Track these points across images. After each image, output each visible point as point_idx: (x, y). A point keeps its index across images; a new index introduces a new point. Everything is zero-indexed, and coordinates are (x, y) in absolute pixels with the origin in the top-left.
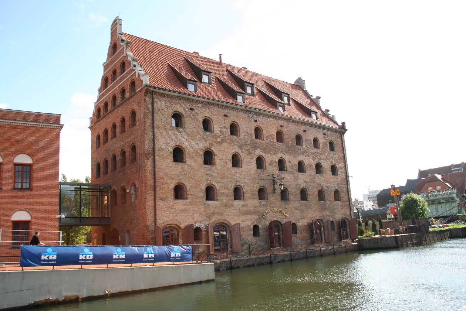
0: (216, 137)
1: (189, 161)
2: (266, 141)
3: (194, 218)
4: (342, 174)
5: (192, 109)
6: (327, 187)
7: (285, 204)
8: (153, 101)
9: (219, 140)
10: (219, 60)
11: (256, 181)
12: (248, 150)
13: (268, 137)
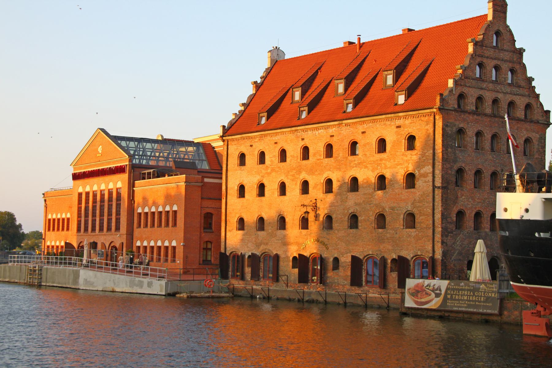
3: (248, 247)
4: (425, 184)
5: (251, 146)
6: (393, 209)
7: (327, 234)
9: (269, 171)
11: (298, 209)
12: (293, 175)
13: (314, 155)
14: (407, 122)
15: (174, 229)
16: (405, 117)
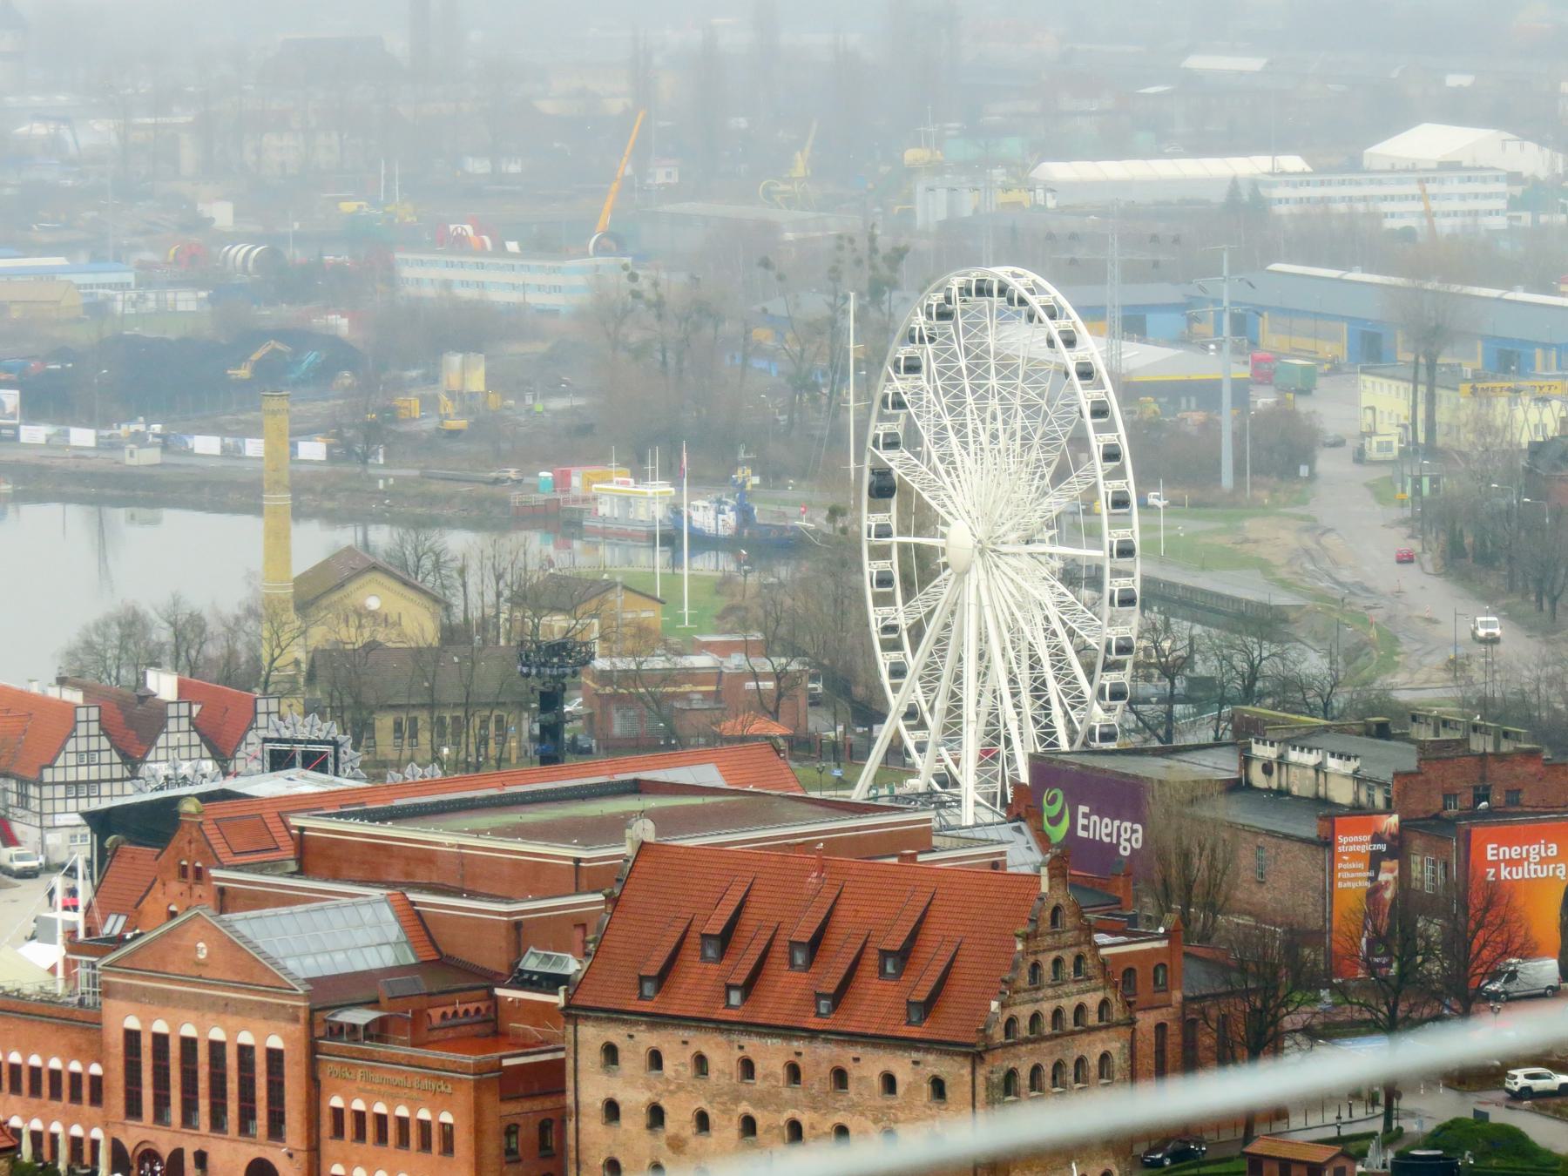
0: (668, 1081)
1: (625, 1121)
2: (759, 1084)
5: (631, 1037)
8: (576, 1031)
12: (724, 1104)
13: (765, 1077)
14: (931, 1058)
15: (447, 1159)
16: (927, 1051)
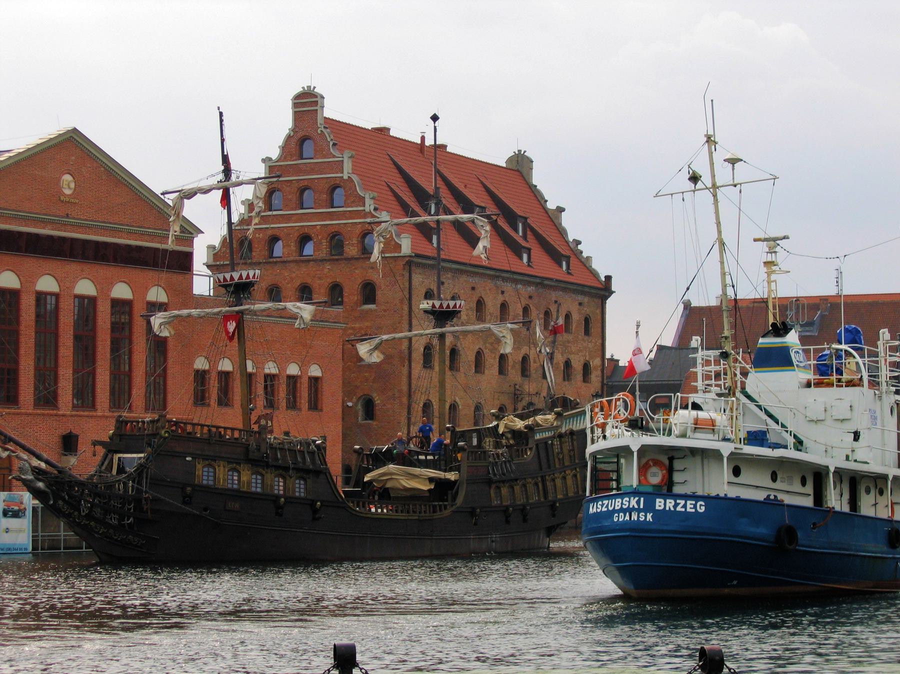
10: (419, 142)
12: (492, 344)
15: (315, 414)
